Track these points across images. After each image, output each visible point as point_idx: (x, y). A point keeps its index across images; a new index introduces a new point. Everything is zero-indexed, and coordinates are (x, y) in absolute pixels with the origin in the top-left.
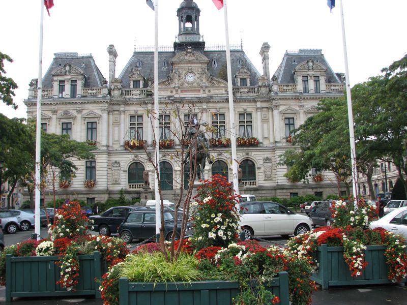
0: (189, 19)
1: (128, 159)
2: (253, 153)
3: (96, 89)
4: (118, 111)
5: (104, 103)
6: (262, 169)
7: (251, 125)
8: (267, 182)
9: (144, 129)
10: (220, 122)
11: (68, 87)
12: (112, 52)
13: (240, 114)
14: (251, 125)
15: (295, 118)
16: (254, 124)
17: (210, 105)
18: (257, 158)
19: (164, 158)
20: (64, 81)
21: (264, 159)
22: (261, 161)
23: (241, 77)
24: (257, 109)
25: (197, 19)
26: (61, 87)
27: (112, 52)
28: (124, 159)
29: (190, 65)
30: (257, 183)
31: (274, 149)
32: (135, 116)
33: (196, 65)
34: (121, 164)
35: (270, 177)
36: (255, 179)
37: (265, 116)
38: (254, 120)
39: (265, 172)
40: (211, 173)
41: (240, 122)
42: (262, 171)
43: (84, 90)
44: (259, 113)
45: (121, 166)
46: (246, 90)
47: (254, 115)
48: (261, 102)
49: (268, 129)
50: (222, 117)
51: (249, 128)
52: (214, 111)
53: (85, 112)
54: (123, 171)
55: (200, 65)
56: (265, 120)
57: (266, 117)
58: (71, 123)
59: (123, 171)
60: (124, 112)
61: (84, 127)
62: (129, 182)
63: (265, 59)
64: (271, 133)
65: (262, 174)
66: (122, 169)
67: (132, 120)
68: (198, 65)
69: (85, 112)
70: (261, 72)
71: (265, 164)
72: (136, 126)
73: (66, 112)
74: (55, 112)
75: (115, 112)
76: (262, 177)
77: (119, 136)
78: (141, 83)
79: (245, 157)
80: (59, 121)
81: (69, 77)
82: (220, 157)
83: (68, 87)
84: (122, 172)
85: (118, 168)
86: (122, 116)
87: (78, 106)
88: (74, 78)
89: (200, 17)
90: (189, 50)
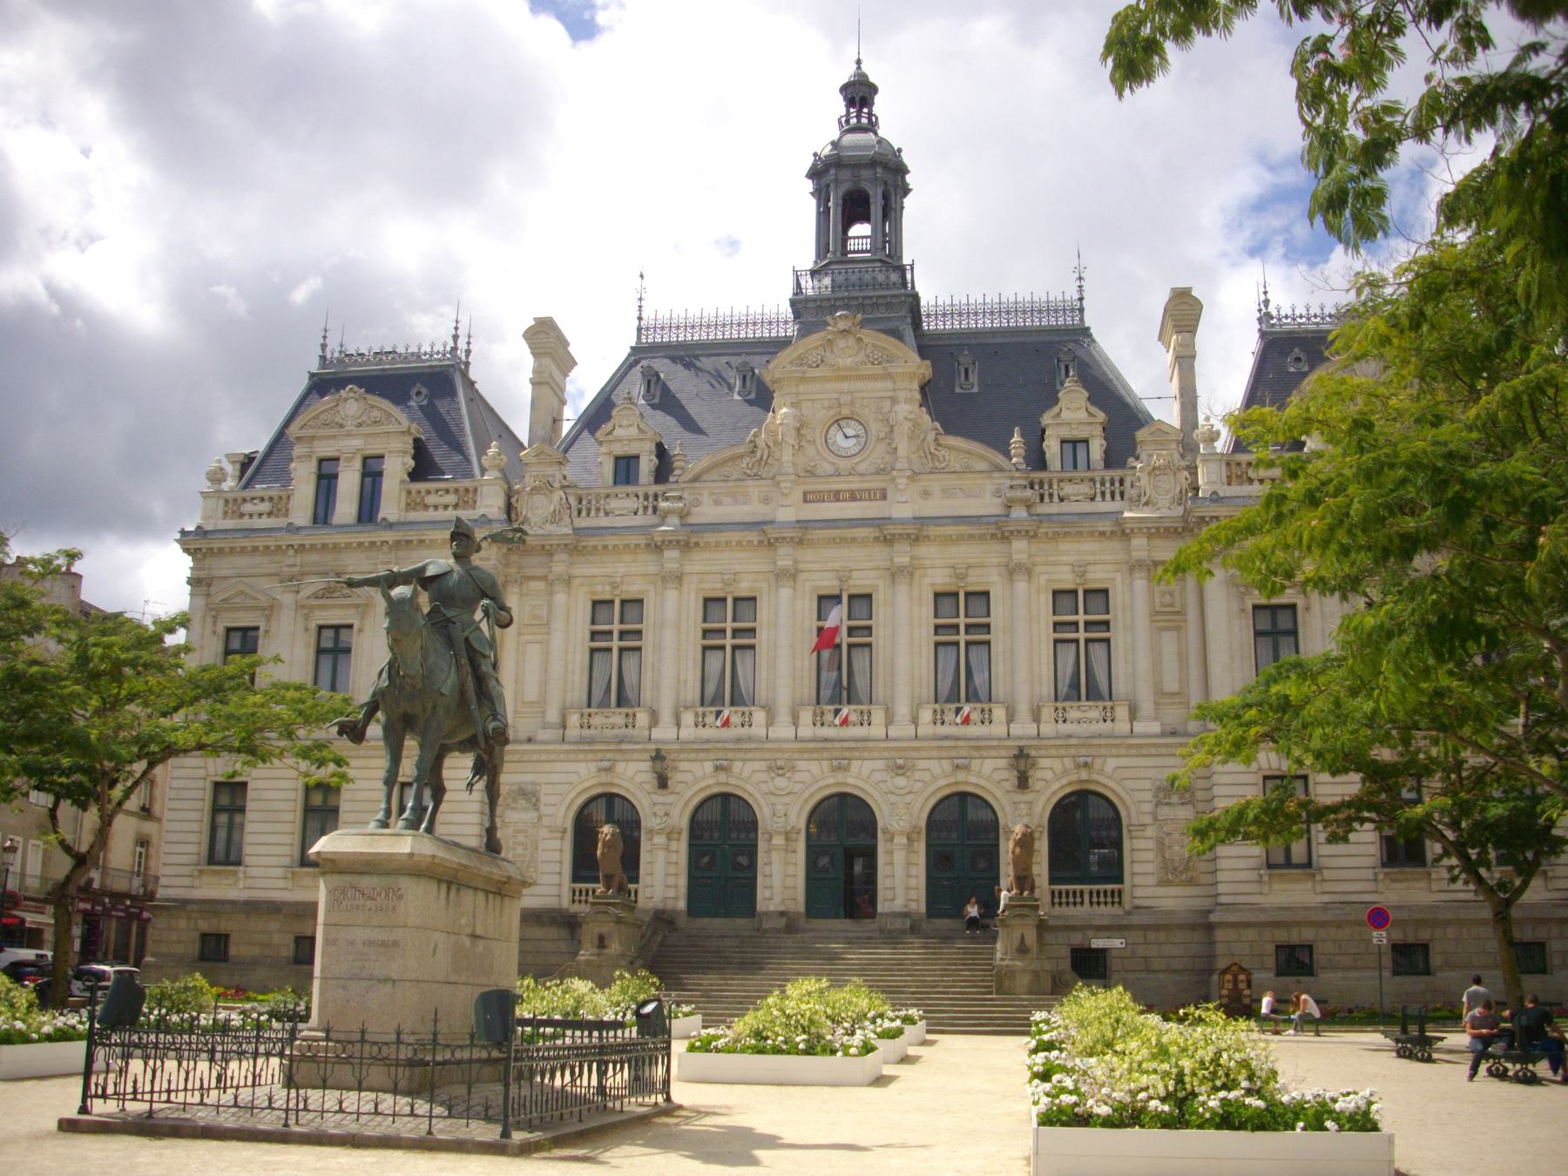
0: (856, 208)
1: (573, 778)
2: (1111, 763)
3: (457, 491)
4: (544, 578)
6: (1150, 832)
7: (1107, 641)
8: (1173, 891)
9: (648, 653)
10: (968, 627)
12: (547, 341)
13: (1056, 593)
14: (1107, 641)
15: (1300, 602)
16: (1118, 636)
17: (926, 551)
18: (1128, 783)
19: (722, 777)
20: (337, 459)
21: (1159, 789)
22: (1148, 796)
23: (1068, 433)
24: (1132, 569)
25: (891, 212)
26: (325, 482)
27: (547, 341)
28: (555, 778)
29: (845, 386)
30: (1126, 898)
32: (612, 602)
33: (871, 385)
34: (544, 799)
35: (1187, 869)
36: (1119, 879)
37: (1167, 598)
38: (1117, 616)
40: (921, 846)
41: (1056, 624)
42: (1151, 844)
43: (409, 492)
44: (1140, 584)
45: (544, 810)
46: (1085, 488)
47: (1116, 599)
48: (1150, 536)
49: (1182, 658)
50: (977, 604)
51: (1098, 651)
52: (940, 579)
54: (551, 829)
55: (890, 385)
56: (1167, 617)
57: (1171, 605)
58: (350, 626)
59: (551, 829)
60: (568, 581)
62: (576, 878)
63: (1185, 361)
64: (1195, 673)
65: (1151, 856)
66: (546, 821)
67: (601, 616)
68: (879, 385)
70: (1167, 413)
71: (1164, 812)
72: (616, 644)
74: (292, 581)
75: (534, 585)
76: (1150, 868)
77: (544, 685)
78: (647, 464)
79: (1074, 777)
80: (307, 618)
81: (357, 443)
82: (961, 776)
84: (544, 833)
85: (531, 816)
86: (560, 598)
87: (381, 557)
89: (908, 201)
90: (842, 325)
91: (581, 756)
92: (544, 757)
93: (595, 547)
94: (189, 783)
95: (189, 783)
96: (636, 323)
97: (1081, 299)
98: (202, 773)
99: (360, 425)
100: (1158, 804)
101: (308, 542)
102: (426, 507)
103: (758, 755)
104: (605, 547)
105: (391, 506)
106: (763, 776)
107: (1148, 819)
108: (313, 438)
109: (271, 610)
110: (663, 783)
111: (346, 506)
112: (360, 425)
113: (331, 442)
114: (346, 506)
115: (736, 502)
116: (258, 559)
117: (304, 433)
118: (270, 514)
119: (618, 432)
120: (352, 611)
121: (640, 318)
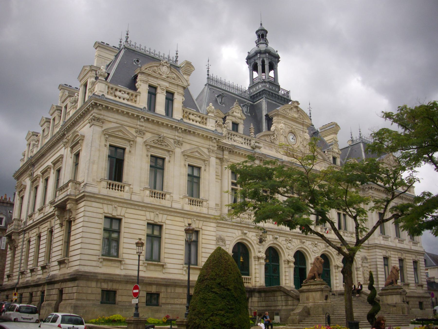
1: (234, 235)
5: (214, 141)
6: (361, 269)
11: (161, 98)
22: (359, 259)
31: (369, 247)
39: (363, 273)
43: (183, 111)
53: (186, 147)
55: (302, 127)
61: (185, 171)
69: (186, 147)
71: (364, 264)
73: (160, 141)
83: (161, 98)
87: (177, 134)
88: (172, 89)
91: (236, 228)
92: (225, 226)
93: (236, 152)
94: (95, 215)
95: (95, 215)
96: (207, 76)
97: (310, 116)
98: (101, 211)
99: (168, 77)
100: (362, 262)
101: (151, 118)
102: (189, 119)
103: (283, 235)
104: (239, 153)
105: (178, 114)
106: (285, 242)
107: (360, 266)
108: (149, 75)
109: (132, 142)
110: (261, 241)
111: (160, 108)
112: (168, 77)
113: (155, 80)
114: (160, 108)
115: (269, 150)
116: (125, 119)
117: (147, 71)
118: (128, 100)
119: (235, 114)
120: (166, 152)
121: (208, 75)
